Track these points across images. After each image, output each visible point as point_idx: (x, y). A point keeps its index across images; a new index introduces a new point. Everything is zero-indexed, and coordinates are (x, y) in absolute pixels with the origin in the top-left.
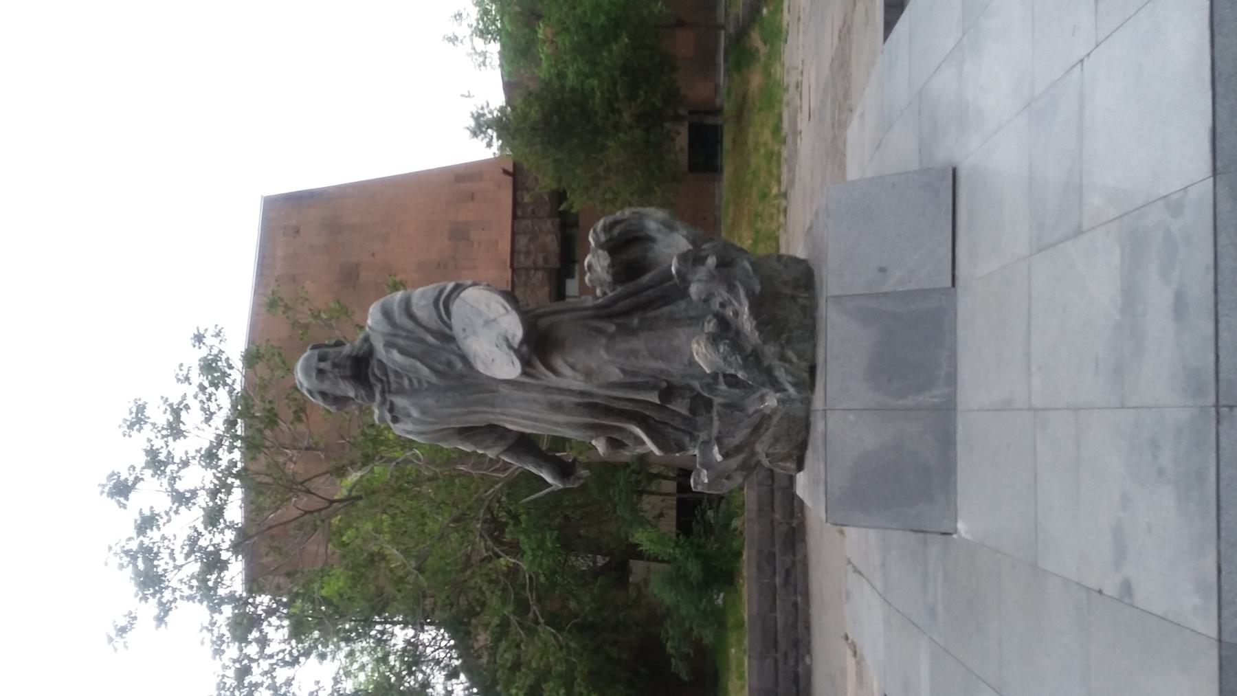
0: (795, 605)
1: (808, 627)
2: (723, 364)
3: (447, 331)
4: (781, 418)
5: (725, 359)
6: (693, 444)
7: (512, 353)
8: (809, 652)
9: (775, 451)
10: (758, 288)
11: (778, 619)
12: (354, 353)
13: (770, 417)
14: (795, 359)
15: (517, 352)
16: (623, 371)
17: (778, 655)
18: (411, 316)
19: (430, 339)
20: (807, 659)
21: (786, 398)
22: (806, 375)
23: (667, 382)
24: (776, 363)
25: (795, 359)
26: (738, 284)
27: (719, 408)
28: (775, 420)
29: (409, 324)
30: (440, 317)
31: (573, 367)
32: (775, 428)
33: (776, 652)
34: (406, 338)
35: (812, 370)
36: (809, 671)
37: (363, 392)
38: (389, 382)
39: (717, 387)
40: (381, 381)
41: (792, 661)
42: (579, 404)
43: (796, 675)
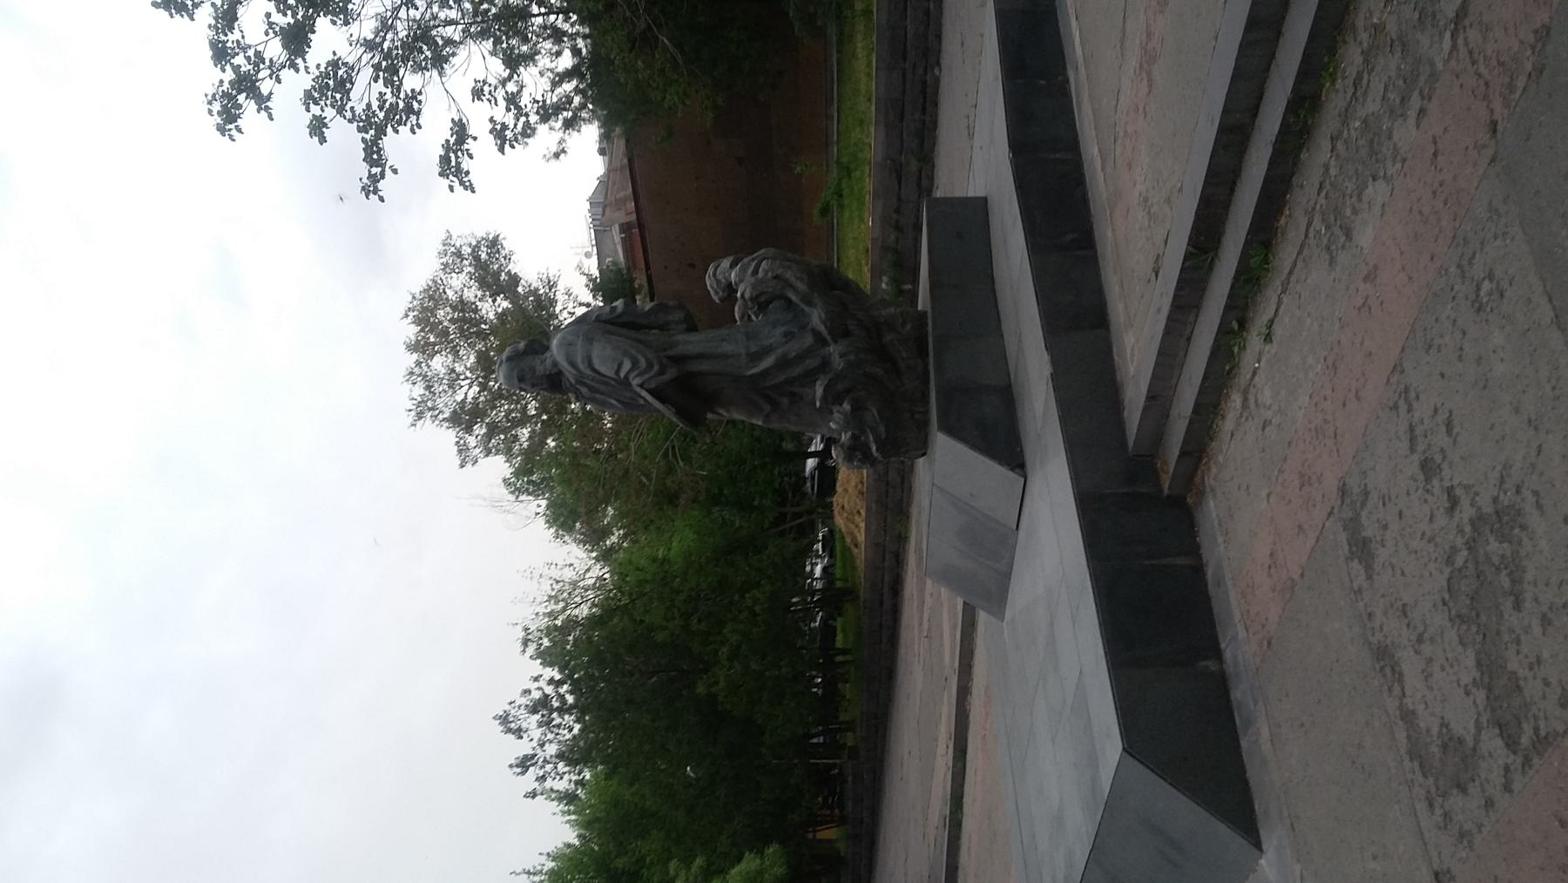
0: (927, 13)
1: (939, 37)
8: (938, 64)
10: (883, 436)
11: (908, 29)
12: (547, 373)
17: (907, 66)
18: (595, 371)
19: (613, 382)
20: (936, 71)
26: (868, 431)
29: (588, 372)
33: (905, 62)
34: (592, 380)
36: (937, 80)
41: (920, 71)
43: (925, 82)
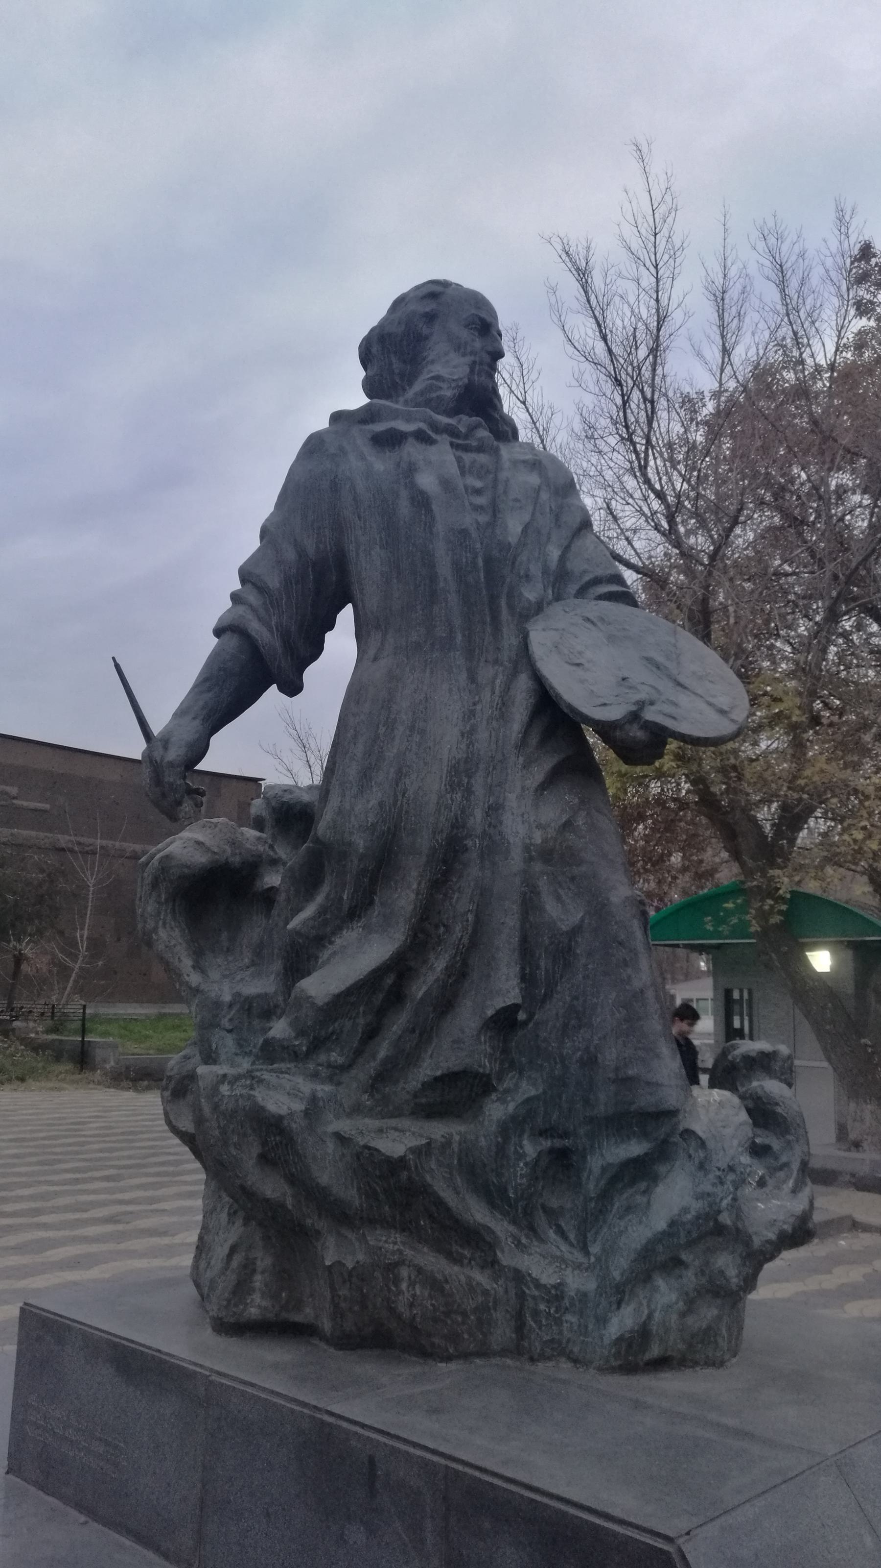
2: (723, 1164)
3: (573, 588)
4: (486, 1293)
5: (731, 1169)
6: (324, 1072)
7: (634, 708)
9: (404, 1286)
13: (491, 1264)
14: (692, 1322)
15: (634, 717)
16: (576, 930)
19: (554, 553)
21: (566, 1302)
22: (655, 1351)
23: (525, 1023)
24: (690, 1278)
25: (692, 1322)
27: (457, 1138)
28: (481, 1278)
30: (597, 581)
31: (568, 825)
32: (463, 1278)
35: (661, 1364)
37: (448, 393)
38: (466, 449)
39: (526, 1136)
40: (466, 437)
42: (458, 823)
